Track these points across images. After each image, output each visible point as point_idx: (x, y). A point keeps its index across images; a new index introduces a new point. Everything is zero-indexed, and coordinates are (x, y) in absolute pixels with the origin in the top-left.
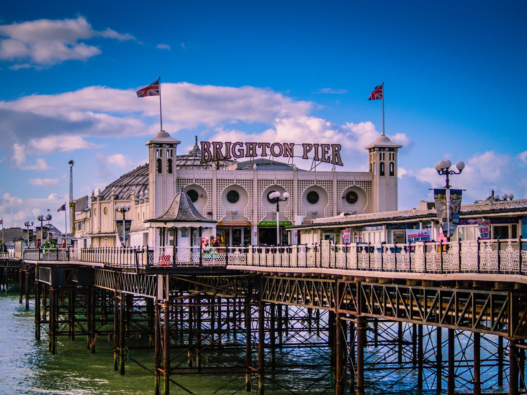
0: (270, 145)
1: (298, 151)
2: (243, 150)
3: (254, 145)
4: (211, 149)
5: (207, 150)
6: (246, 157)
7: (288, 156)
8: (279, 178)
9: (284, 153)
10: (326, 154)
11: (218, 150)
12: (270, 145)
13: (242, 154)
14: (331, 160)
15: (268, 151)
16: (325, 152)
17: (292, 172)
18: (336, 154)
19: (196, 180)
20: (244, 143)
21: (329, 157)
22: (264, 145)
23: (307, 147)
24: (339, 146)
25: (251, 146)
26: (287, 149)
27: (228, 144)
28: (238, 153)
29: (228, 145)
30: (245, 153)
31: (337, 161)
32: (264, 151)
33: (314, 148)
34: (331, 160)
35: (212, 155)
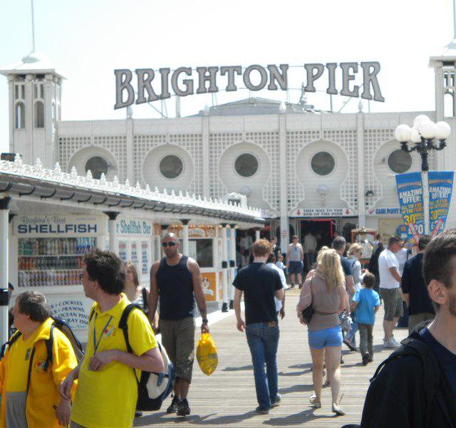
0: (243, 71)
1: (297, 78)
2: (192, 81)
3: (213, 71)
4: (134, 83)
5: (127, 85)
6: (198, 93)
7: (276, 89)
8: (249, 129)
9: (268, 83)
10: (350, 81)
11: (147, 84)
12: (243, 71)
13: (190, 87)
14: (361, 91)
15: (239, 80)
16: (347, 78)
17: (274, 117)
19: (247, 134)
20: (194, 68)
21: (356, 88)
22: (231, 70)
23: (313, 71)
24: (376, 65)
25: (207, 74)
26: (277, 76)
27: (164, 72)
28: (183, 88)
29: (165, 73)
30: (196, 86)
31: (372, 93)
32: (231, 80)
33: (326, 71)
34: (361, 91)
35: (136, 90)
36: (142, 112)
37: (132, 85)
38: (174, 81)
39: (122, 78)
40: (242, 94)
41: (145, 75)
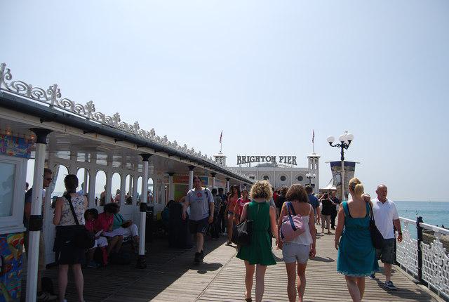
15: (265, 159)
16: (289, 160)
18: (294, 160)
23: (281, 158)
26: (274, 158)
27: (248, 157)
36: (243, 165)
37: (241, 160)
38: (250, 160)
39: (239, 158)
40: (266, 162)
41: (244, 158)
